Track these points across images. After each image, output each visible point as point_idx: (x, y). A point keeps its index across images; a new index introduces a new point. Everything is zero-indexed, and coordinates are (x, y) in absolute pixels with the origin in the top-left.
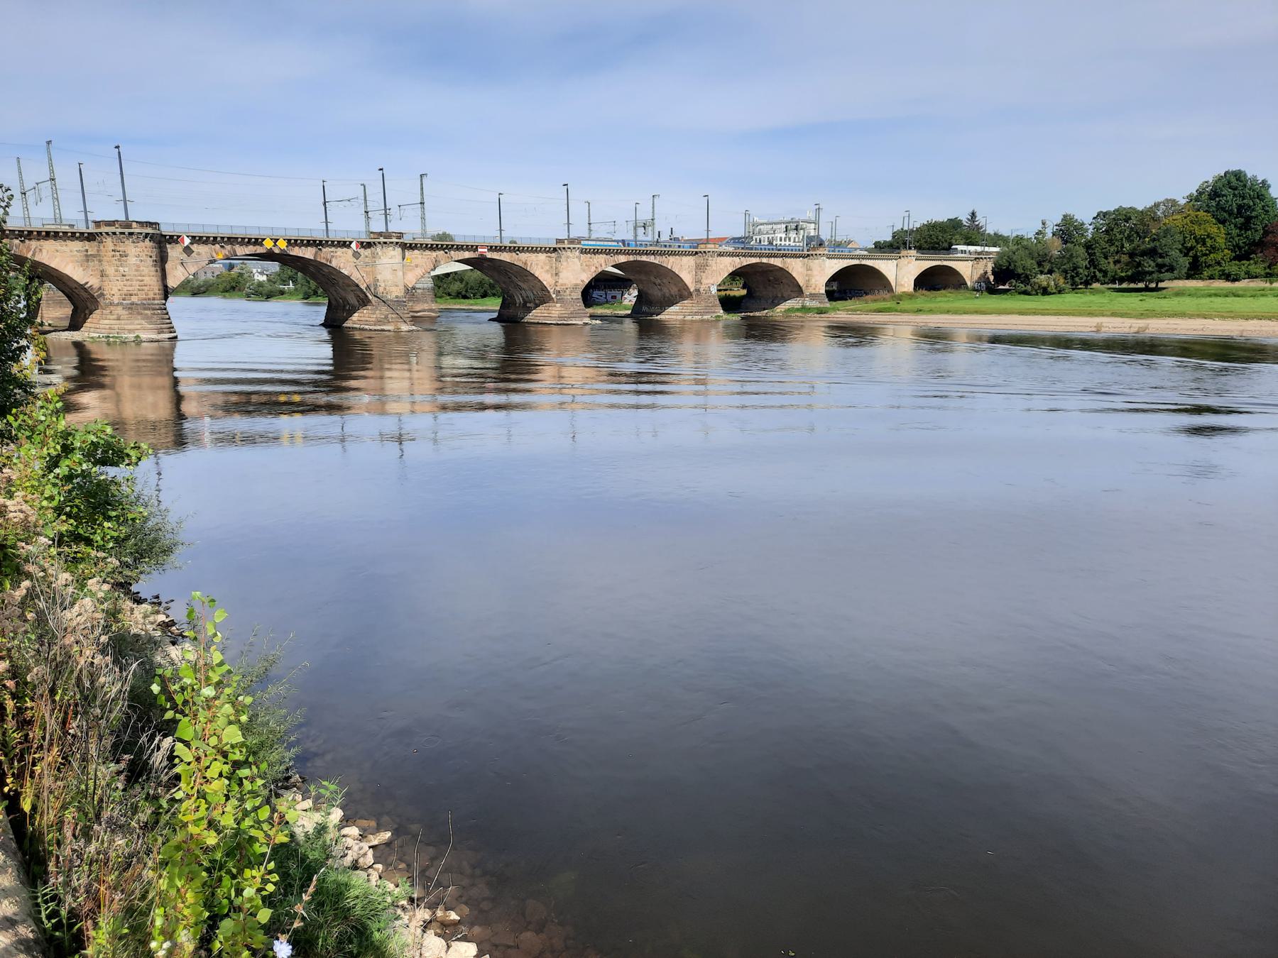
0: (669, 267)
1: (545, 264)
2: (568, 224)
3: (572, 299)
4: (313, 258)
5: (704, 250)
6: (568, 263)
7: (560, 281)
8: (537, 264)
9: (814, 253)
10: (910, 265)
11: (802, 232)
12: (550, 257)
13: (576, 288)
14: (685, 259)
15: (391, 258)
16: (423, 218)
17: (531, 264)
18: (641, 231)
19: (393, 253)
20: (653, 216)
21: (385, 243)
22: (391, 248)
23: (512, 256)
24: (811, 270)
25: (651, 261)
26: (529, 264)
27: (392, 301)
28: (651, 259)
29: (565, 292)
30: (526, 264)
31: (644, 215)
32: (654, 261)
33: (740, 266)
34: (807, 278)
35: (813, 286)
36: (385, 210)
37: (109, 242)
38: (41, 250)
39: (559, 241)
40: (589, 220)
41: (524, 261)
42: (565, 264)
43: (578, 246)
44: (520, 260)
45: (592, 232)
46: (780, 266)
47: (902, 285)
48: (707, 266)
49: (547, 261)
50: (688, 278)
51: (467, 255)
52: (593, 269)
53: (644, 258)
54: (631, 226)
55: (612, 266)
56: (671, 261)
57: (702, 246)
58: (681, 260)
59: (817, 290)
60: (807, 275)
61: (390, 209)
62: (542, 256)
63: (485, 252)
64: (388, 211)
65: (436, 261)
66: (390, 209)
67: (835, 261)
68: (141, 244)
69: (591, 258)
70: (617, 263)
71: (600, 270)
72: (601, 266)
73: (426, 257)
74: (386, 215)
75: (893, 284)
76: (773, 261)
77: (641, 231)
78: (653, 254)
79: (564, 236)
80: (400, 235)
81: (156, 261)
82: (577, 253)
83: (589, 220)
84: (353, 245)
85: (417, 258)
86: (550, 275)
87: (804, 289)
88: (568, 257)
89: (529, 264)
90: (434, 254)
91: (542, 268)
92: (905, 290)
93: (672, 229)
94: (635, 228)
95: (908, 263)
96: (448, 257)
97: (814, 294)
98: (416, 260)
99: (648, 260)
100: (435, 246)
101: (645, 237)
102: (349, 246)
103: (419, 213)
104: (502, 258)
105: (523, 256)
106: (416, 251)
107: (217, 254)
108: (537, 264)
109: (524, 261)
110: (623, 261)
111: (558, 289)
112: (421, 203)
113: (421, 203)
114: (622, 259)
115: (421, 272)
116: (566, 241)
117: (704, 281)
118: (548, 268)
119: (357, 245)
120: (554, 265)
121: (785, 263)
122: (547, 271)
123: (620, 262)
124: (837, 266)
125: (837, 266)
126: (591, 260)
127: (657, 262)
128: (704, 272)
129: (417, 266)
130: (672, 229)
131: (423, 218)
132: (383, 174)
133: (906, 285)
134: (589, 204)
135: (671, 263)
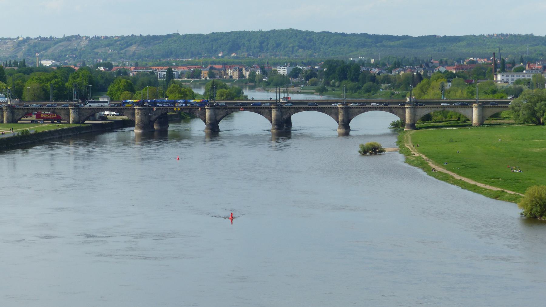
4: (188, 112)
8: (265, 113)
12: (270, 110)
26: (261, 113)
37: (136, 110)
38: (124, 112)
52: (289, 114)
62: (267, 110)
65: (227, 113)
68: (142, 111)
69: (287, 110)
81: (146, 115)
84: (199, 109)
90: (227, 111)
91: (267, 114)
102: (197, 108)
106: (220, 110)
107: (163, 112)
108: (265, 113)
118: (269, 114)
119: (200, 109)
122: (269, 115)
129: (220, 114)
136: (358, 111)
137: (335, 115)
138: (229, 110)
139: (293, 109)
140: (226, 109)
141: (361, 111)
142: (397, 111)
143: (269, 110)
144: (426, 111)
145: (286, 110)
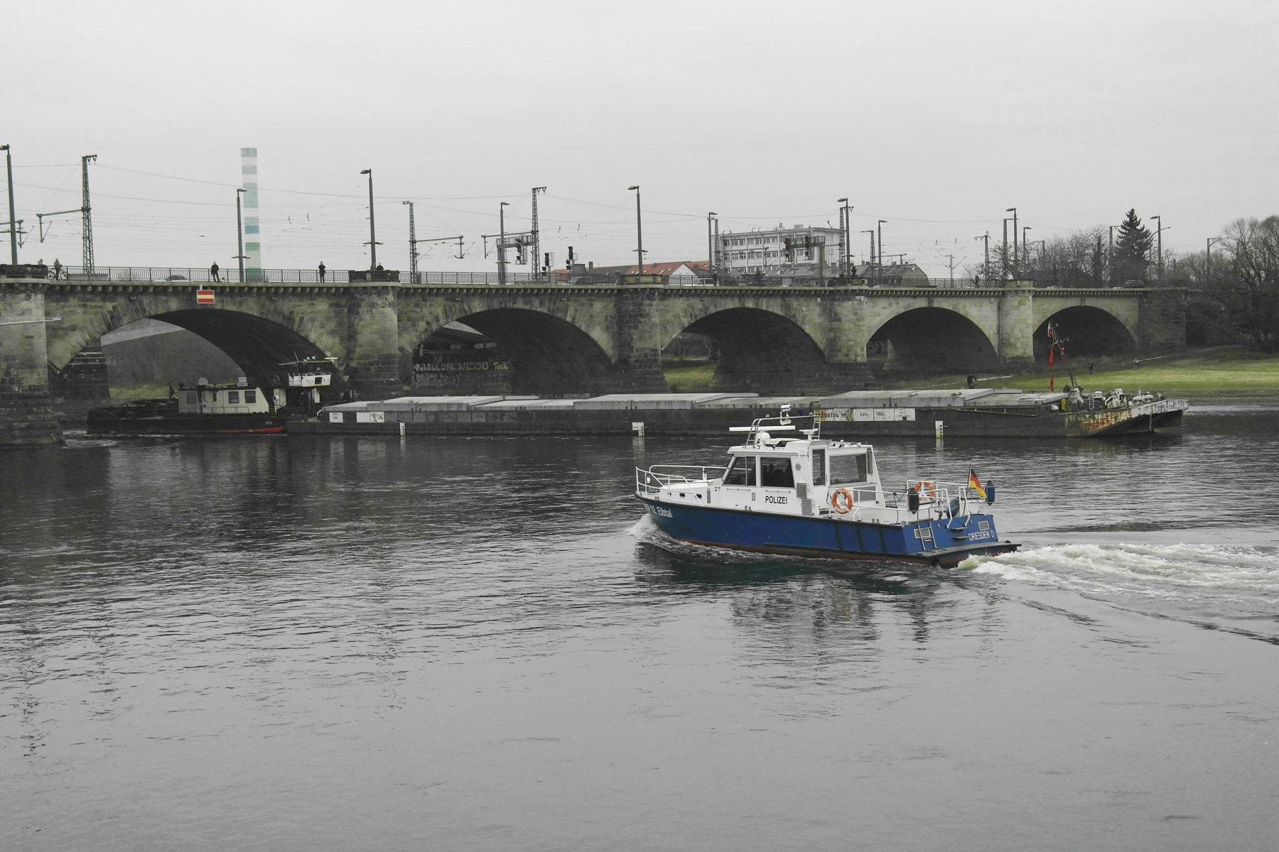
0: (569, 319)
1: (328, 319)
2: (373, 243)
3: (382, 383)
5: (634, 286)
6: (373, 316)
7: (358, 350)
9: (842, 288)
10: (1023, 308)
11: (816, 250)
12: (338, 305)
13: (389, 363)
14: (598, 306)
15: (23, 314)
16: (87, 238)
17: (302, 319)
18: (511, 254)
19: (25, 304)
20: (535, 224)
21: (11, 286)
22: (22, 296)
23: (263, 306)
24: (839, 320)
25: (534, 309)
26: (297, 319)
27: (21, 397)
28: (536, 306)
29: (368, 370)
30: (290, 318)
31: (518, 225)
32: (539, 310)
33: (702, 315)
34: (832, 335)
35: (845, 350)
36: (12, 222)
39: (354, 275)
40: (413, 235)
41: (287, 313)
42: (367, 317)
43: (392, 284)
44: (280, 313)
45: (418, 258)
46: (780, 313)
47: (1011, 345)
48: (641, 315)
49: (334, 315)
50: (600, 336)
51: (174, 305)
52: (422, 325)
53: (520, 305)
54: (492, 246)
55: (457, 320)
56: (571, 309)
57: (631, 280)
58: (591, 305)
59: (852, 357)
60: (831, 330)
61: (20, 222)
62: (322, 306)
63: (211, 300)
64: (17, 225)
65: (112, 318)
66: (20, 222)
67: (882, 303)
69: (417, 305)
70: (468, 313)
71: (435, 327)
72: (437, 320)
73: (94, 310)
74: (13, 232)
75: (994, 341)
76: (764, 305)
77: (511, 254)
78: (537, 295)
79: (365, 266)
80: (40, 270)
82: (391, 298)
83: (413, 235)
85: (73, 312)
86: (337, 339)
87: (826, 353)
88: (373, 305)
89: (297, 319)
90: (109, 306)
91: (322, 326)
92: (1019, 353)
93: (571, 248)
94: (501, 250)
95: (1020, 303)
96: (137, 310)
97: (846, 364)
98: (73, 317)
99: (527, 307)
100: (111, 289)
101: (520, 270)
103: (80, 227)
104: (244, 309)
105: (287, 305)
106: (73, 301)
108: (313, 320)
109: (287, 313)
110: (478, 310)
111: (353, 364)
112: (83, 210)
113: (83, 210)
114: (478, 306)
115: (81, 340)
116: (369, 276)
117: (637, 345)
118: (332, 325)
120: (346, 320)
121: (787, 307)
122: (332, 333)
123: (474, 311)
124: (887, 312)
125: (887, 312)
126: (418, 310)
127: (545, 311)
128: (636, 328)
129: (73, 328)
130: (571, 248)
131: (87, 238)
132: (9, 157)
133: (1019, 345)
134: (411, 205)
135: (572, 313)
136: (686, 311)
137: (607, 328)
138: (121, 301)
139: (441, 300)
140: (104, 300)
141: (693, 308)
142: (804, 309)
143: (331, 305)
144: (885, 308)
145: (413, 301)
